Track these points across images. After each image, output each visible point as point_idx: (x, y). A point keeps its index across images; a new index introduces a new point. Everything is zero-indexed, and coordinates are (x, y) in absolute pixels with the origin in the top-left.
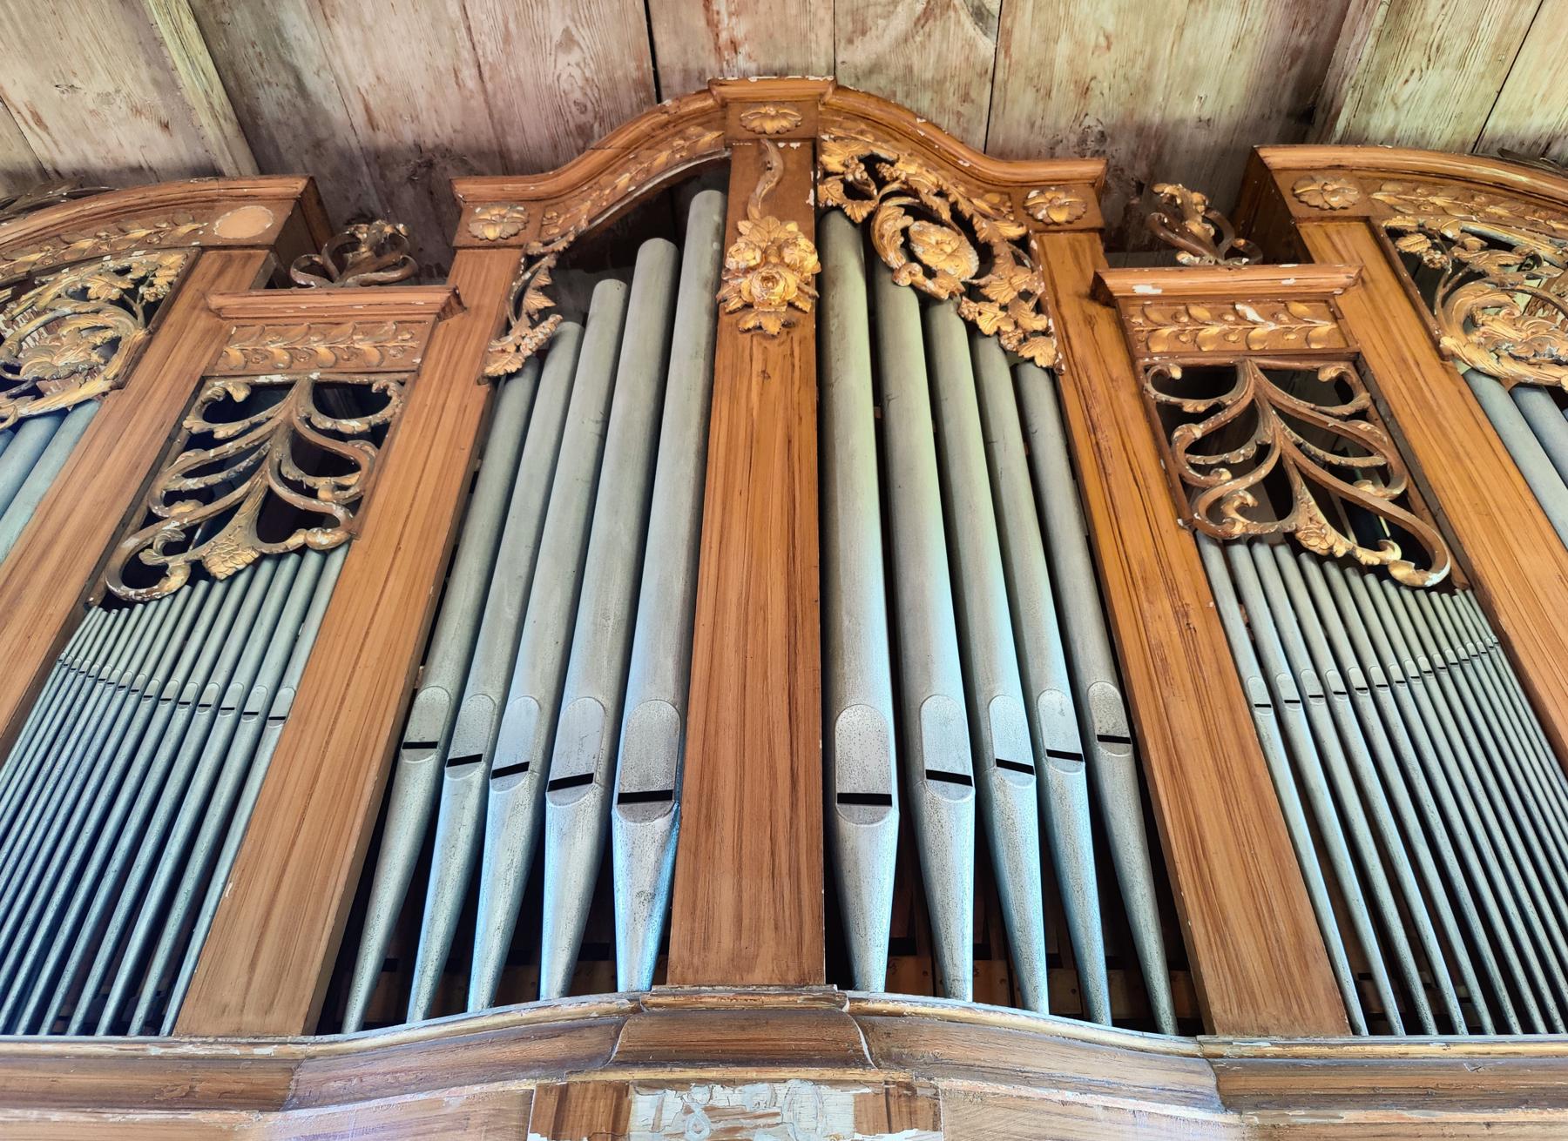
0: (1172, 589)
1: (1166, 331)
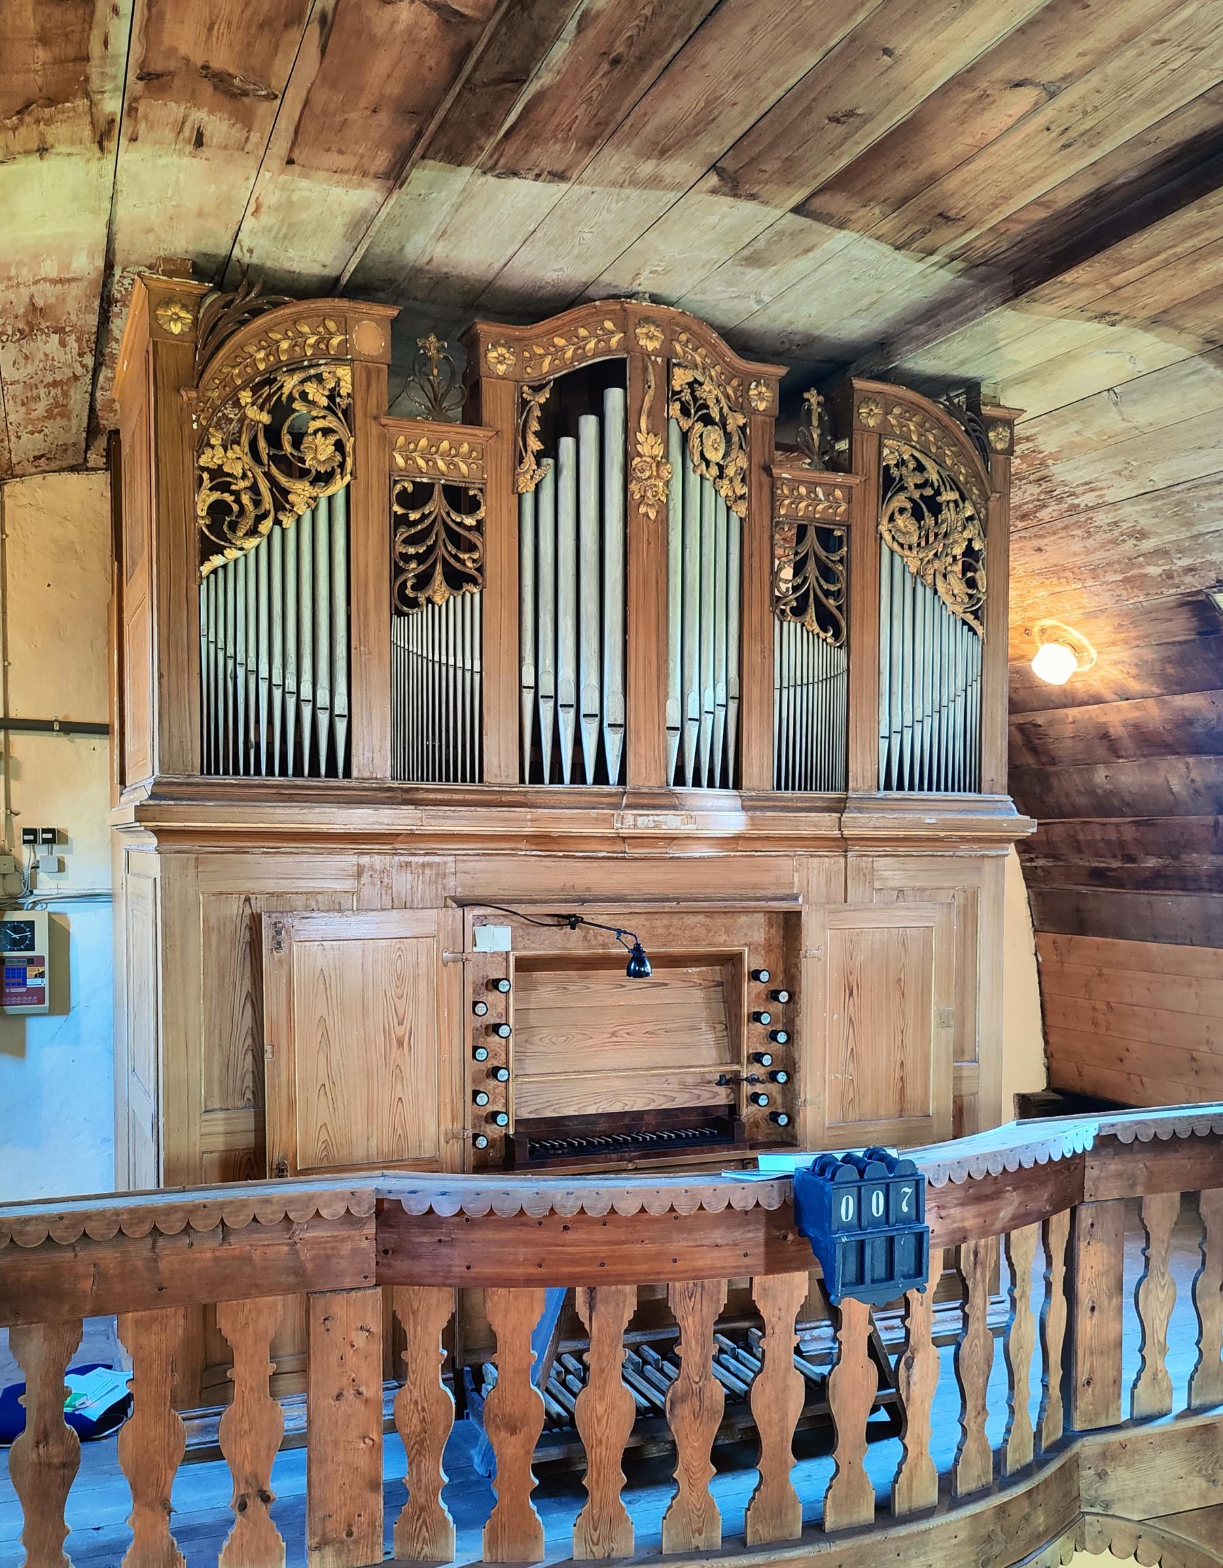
0: (762, 641)
1: (786, 502)
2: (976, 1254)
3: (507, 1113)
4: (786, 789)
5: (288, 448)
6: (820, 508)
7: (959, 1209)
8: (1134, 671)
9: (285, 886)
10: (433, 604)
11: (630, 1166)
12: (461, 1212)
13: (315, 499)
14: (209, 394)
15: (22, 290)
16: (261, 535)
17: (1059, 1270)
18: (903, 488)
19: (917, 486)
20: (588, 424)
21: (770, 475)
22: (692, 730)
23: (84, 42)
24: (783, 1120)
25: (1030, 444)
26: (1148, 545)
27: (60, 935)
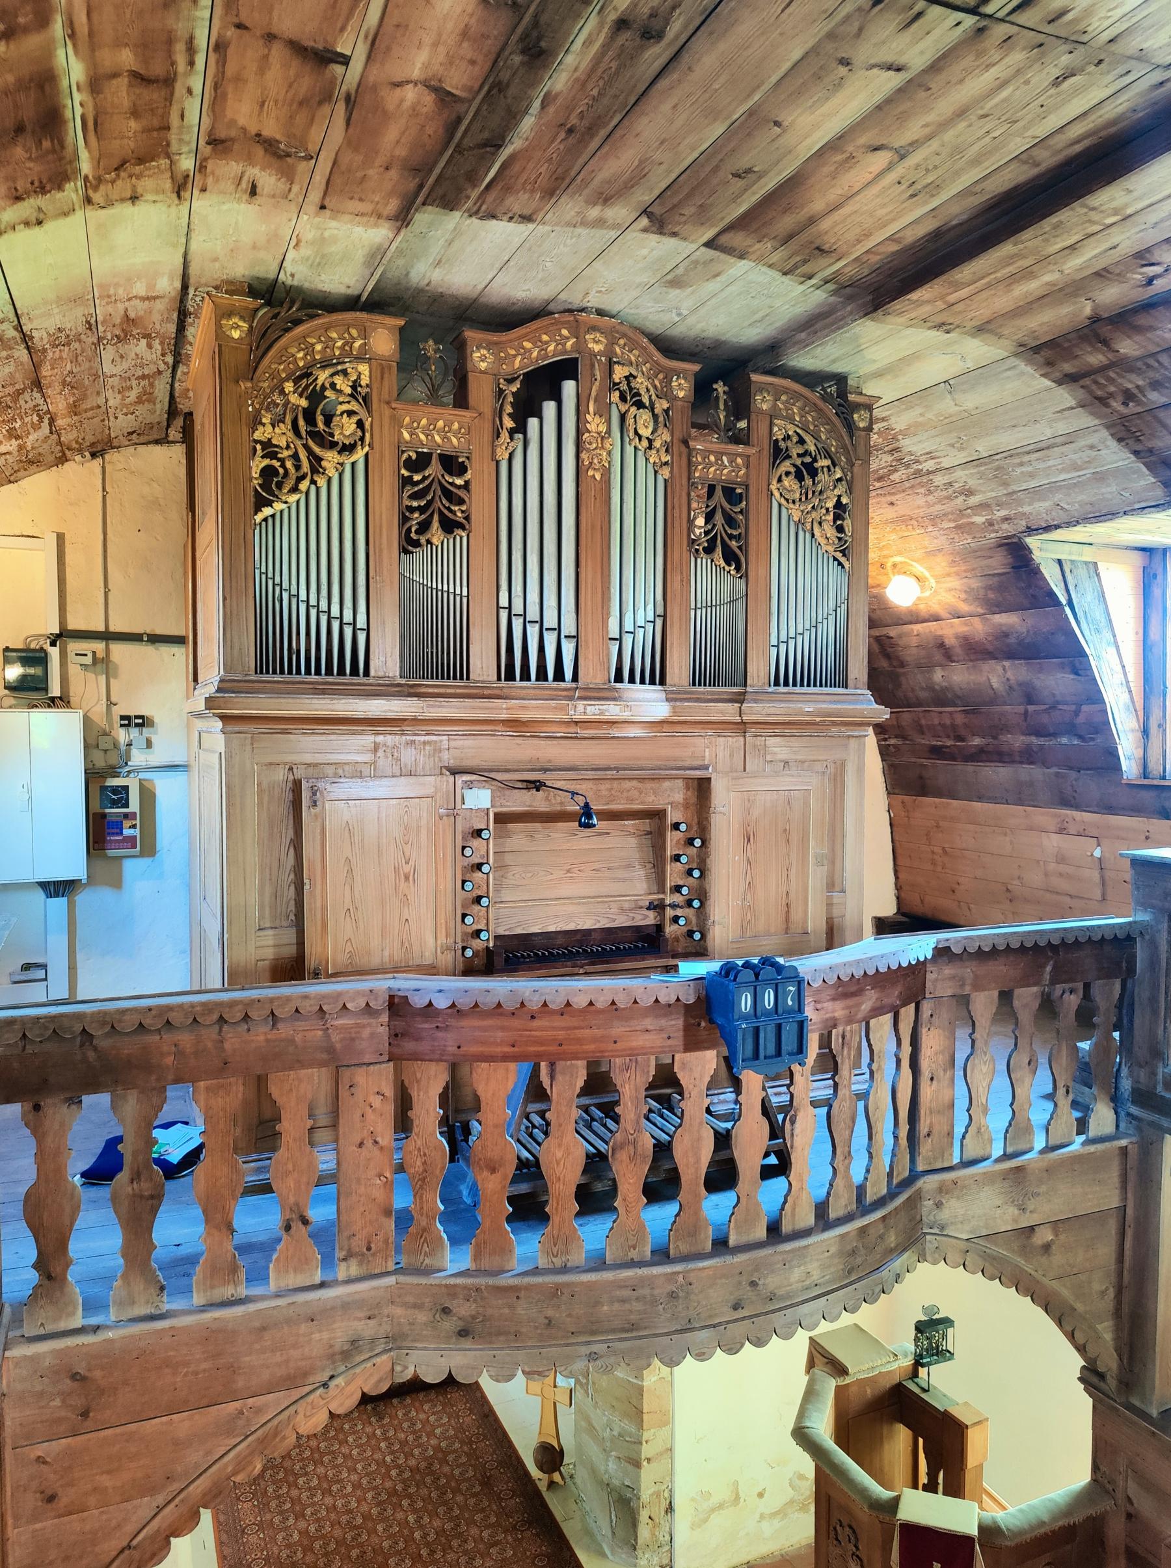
2: (843, 1037)
3: (487, 931)
4: (700, 685)
5: (321, 425)
6: (725, 471)
7: (830, 1003)
8: (963, 596)
9: (319, 758)
10: (432, 544)
11: (581, 971)
12: (453, 1005)
13: (342, 464)
14: (261, 384)
15: (119, 304)
16: (301, 492)
17: (907, 1049)
18: (789, 457)
19: (799, 455)
20: (549, 408)
21: (688, 446)
22: (628, 640)
23: (166, 115)
24: (697, 936)
25: (885, 424)
26: (974, 500)
27: (148, 796)
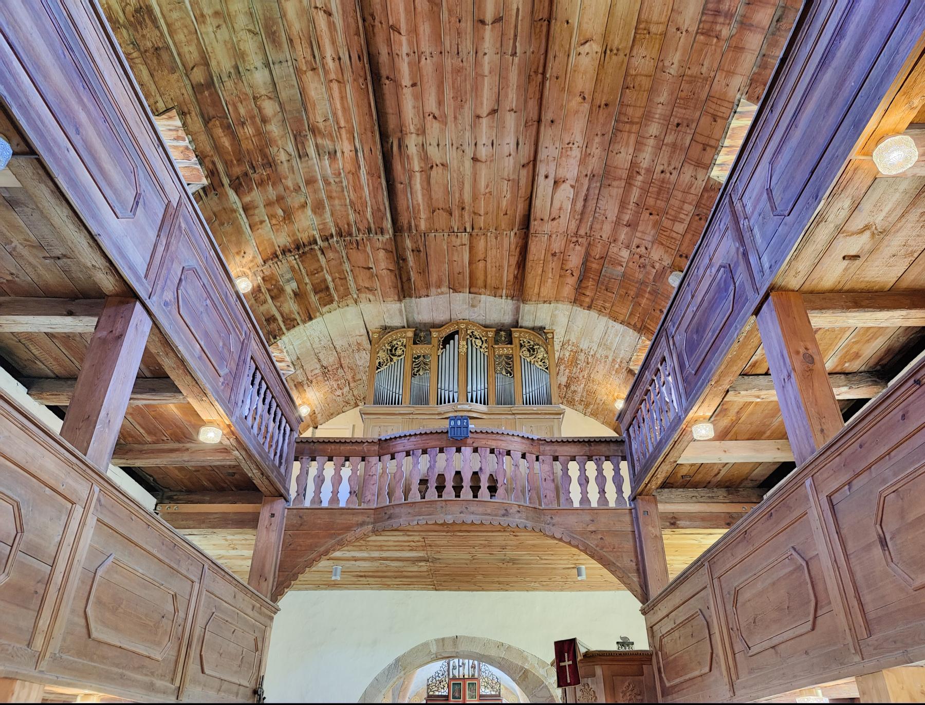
20: (452, 342)
